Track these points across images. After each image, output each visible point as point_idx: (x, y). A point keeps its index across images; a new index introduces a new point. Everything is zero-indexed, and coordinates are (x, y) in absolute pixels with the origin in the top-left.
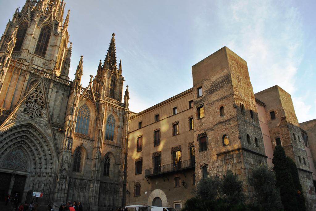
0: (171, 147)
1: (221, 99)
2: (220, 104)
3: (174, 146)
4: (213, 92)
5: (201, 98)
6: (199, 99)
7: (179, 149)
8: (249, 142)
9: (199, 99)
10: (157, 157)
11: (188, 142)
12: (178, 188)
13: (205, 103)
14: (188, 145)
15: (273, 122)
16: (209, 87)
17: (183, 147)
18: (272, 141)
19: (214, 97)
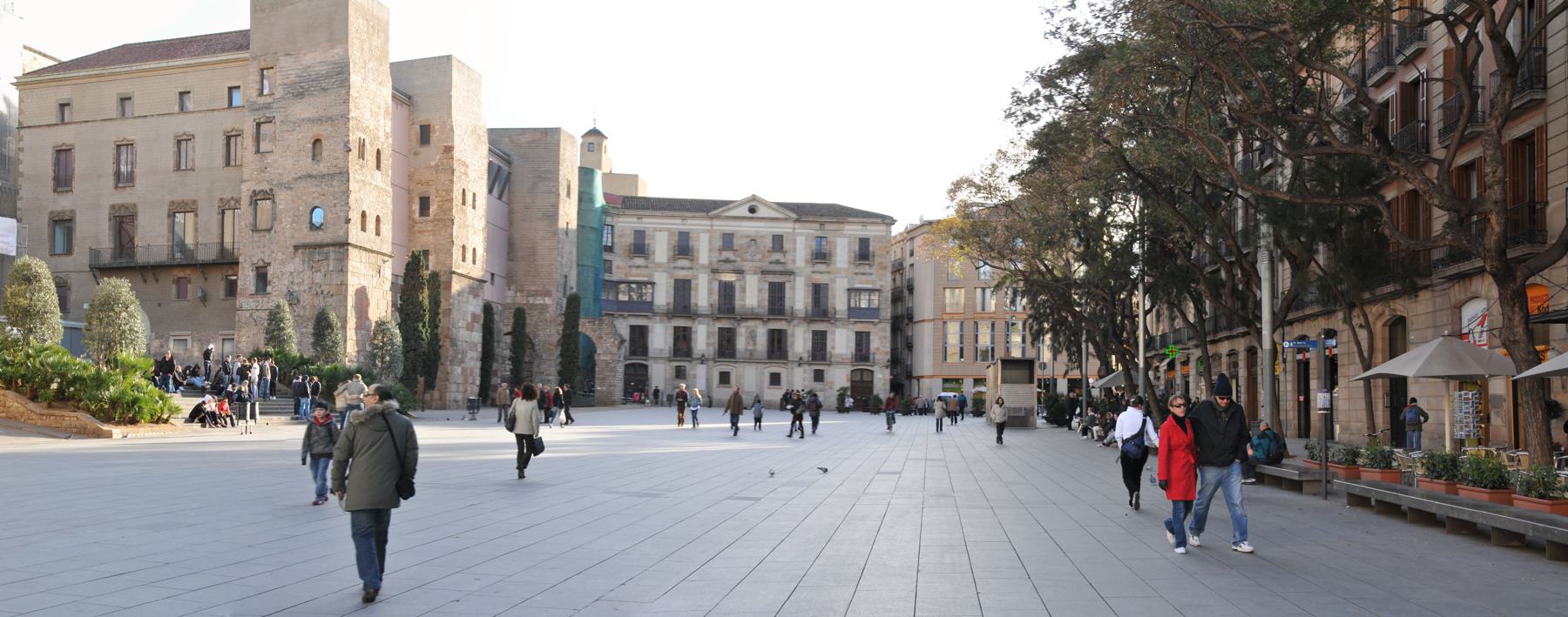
0: (168, 198)
1: (319, 120)
2: (316, 130)
3: (178, 197)
4: (301, 95)
5: (269, 100)
6: (261, 100)
7: (188, 207)
8: (363, 229)
9: (261, 100)
10: (123, 222)
11: (218, 195)
12: (184, 304)
13: (279, 118)
14: (217, 204)
15: (424, 150)
16: (292, 78)
17: (201, 205)
18: (410, 202)
19: (302, 109)
